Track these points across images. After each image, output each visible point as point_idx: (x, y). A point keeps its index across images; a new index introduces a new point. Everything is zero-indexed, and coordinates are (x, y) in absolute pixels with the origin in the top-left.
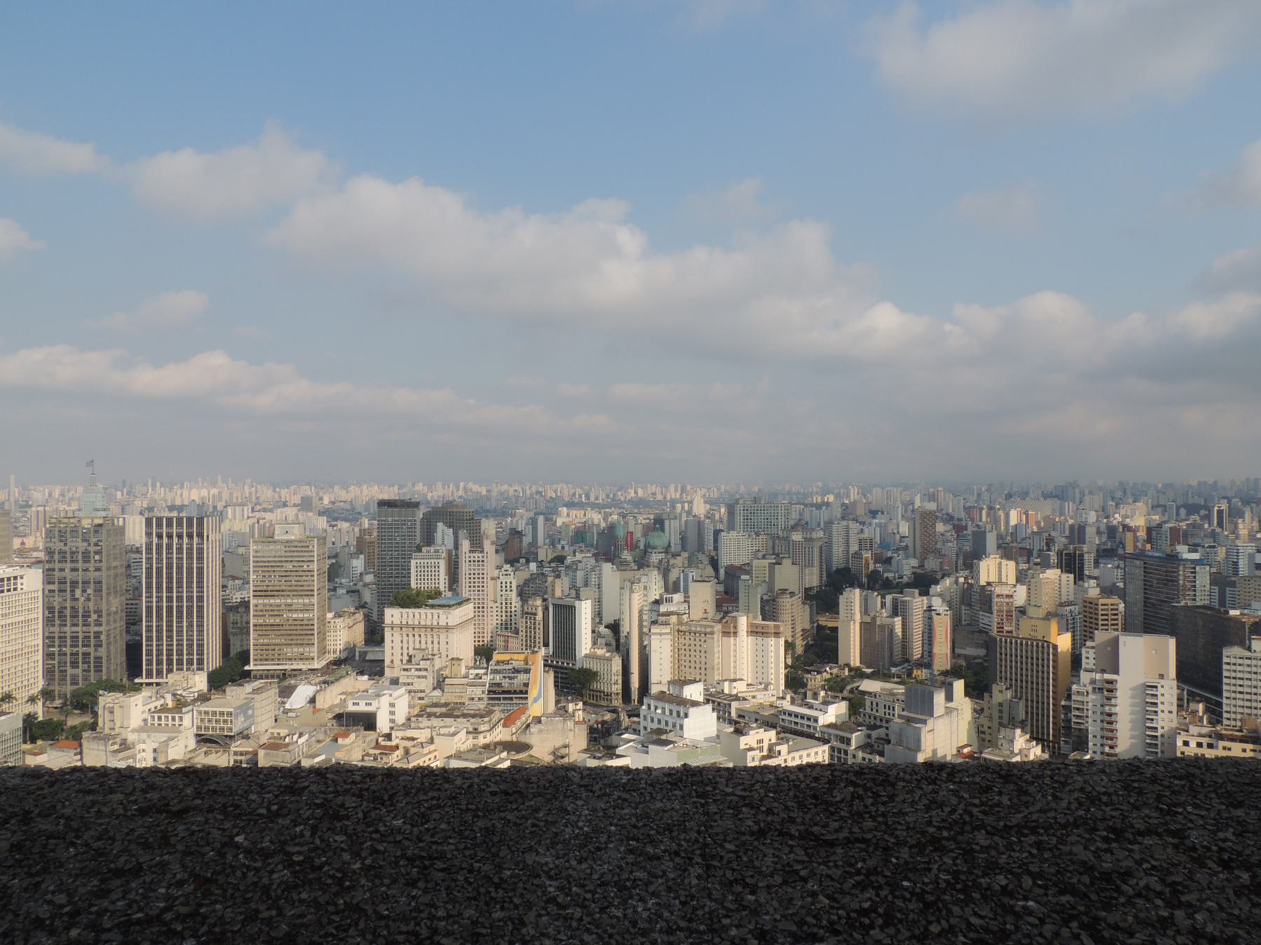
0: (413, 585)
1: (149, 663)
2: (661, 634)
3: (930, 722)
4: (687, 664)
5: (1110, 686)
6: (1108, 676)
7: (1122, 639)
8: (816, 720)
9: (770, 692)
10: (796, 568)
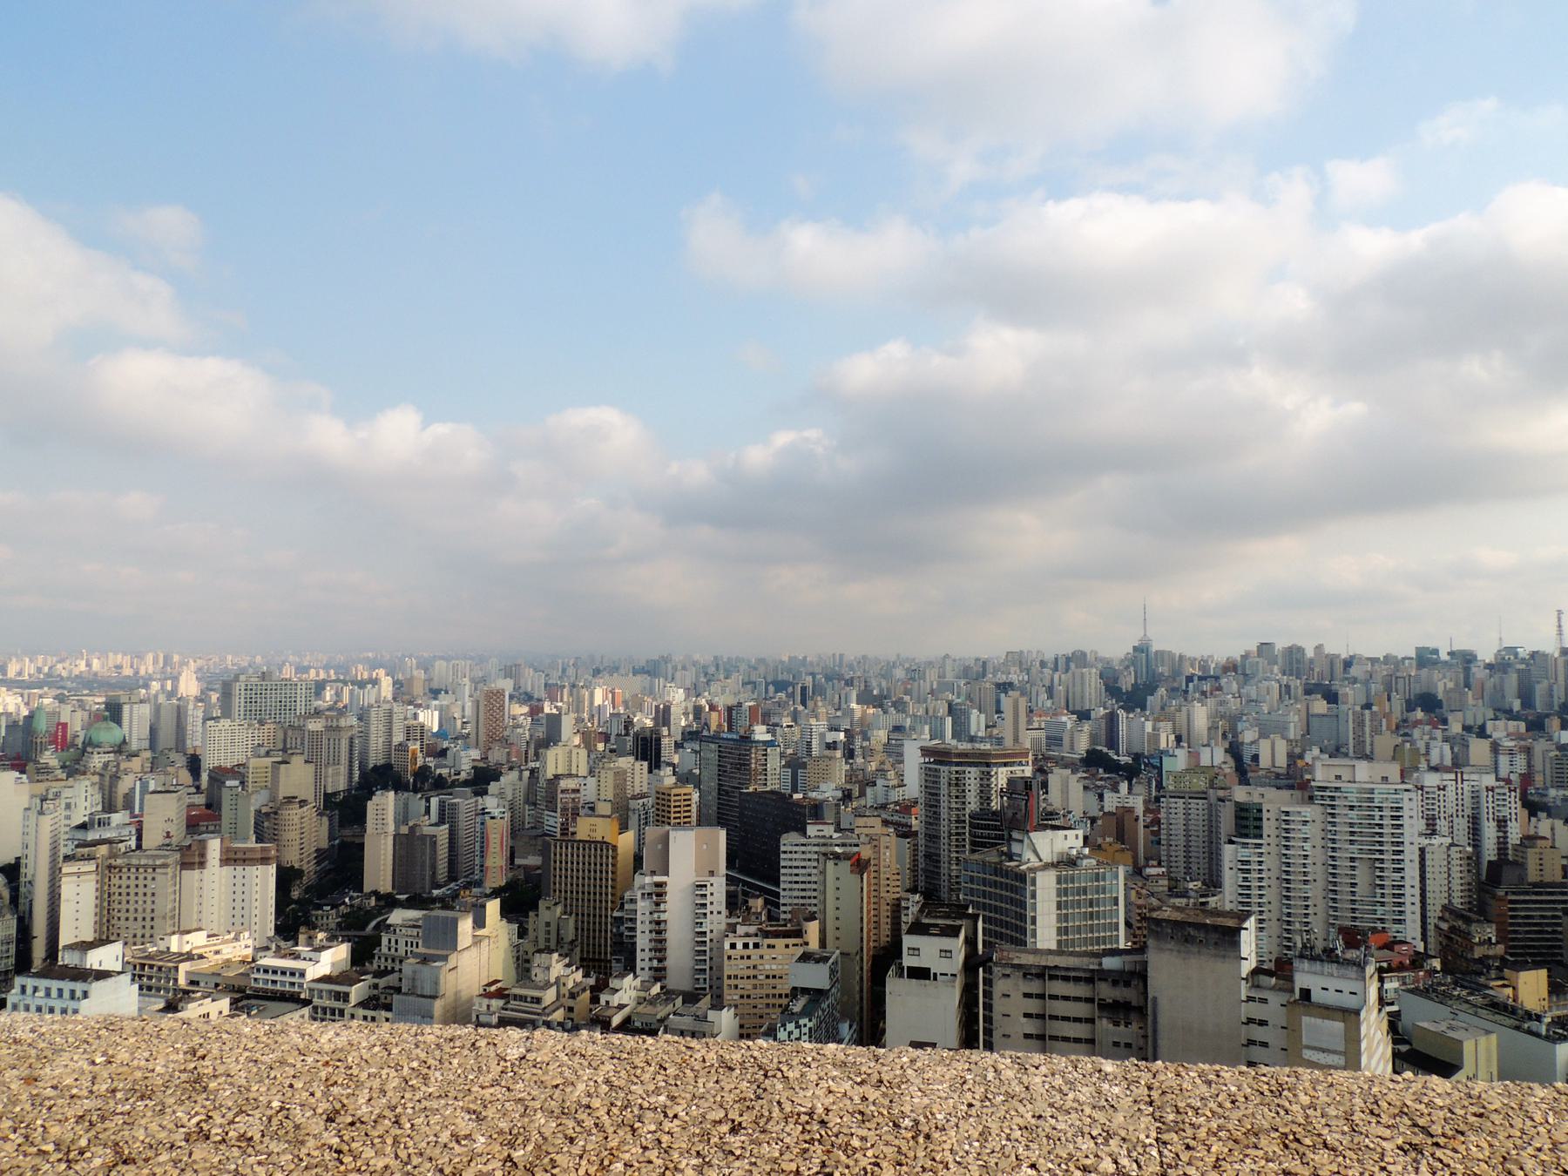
2: (78, 875)
3: (453, 959)
4: (123, 915)
5: (659, 890)
6: (657, 879)
7: (672, 834)
8: (302, 975)
9: (243, 943)
10: (311, 768)
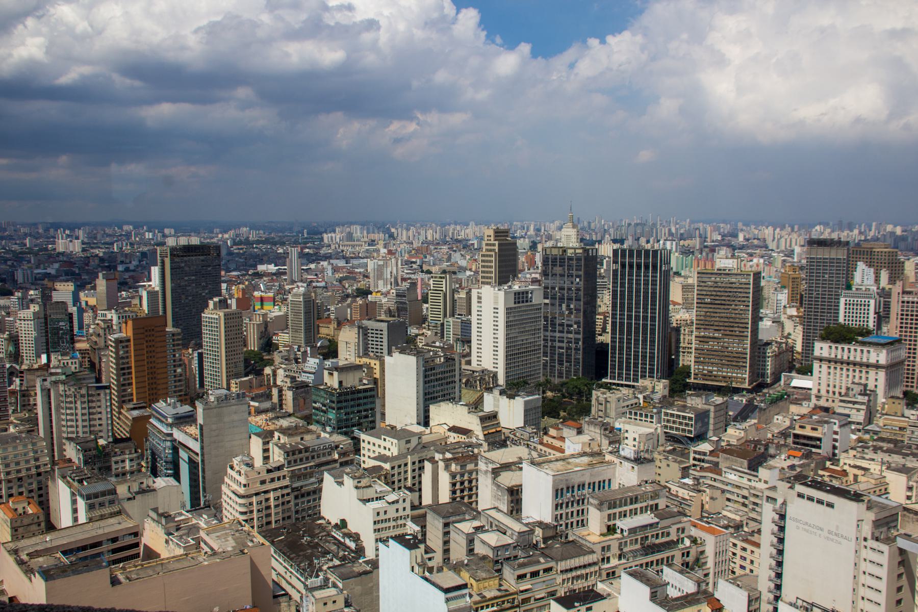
0: (841, 320)
1: (613, 367)
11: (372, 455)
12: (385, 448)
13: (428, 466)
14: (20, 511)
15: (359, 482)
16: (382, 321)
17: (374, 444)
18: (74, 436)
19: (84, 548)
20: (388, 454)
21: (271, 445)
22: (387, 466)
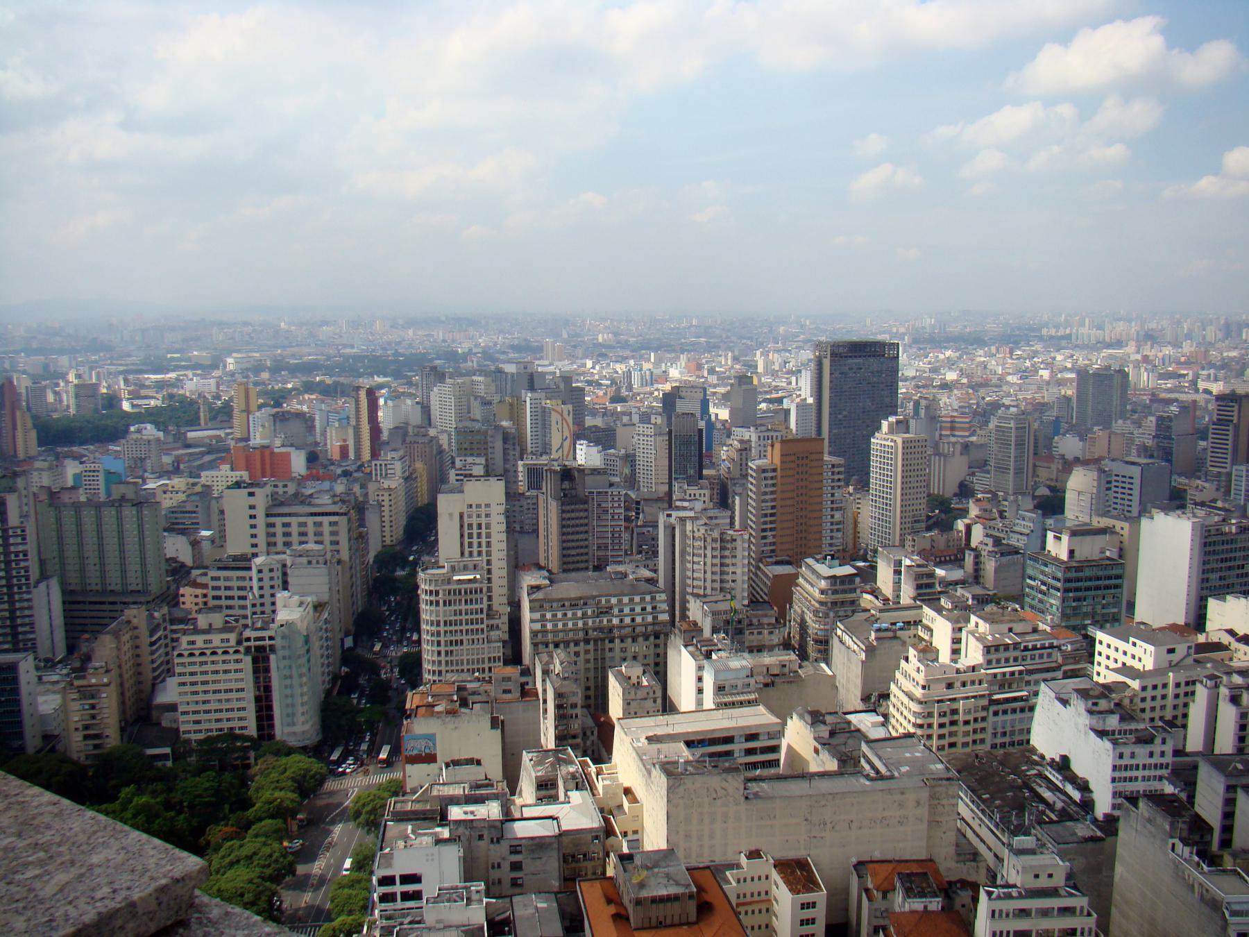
11: (1112, 665)
12: (1133, 657)
13: (1201, 693)
14: (634, 680)
15: (1095, 704)
16: (1133, 463)
17: (1117, 650)
18: (702, 592)
19: (713, 741)
20: (1138, 666)
21: (964, 635)
22: (1135, 684)
